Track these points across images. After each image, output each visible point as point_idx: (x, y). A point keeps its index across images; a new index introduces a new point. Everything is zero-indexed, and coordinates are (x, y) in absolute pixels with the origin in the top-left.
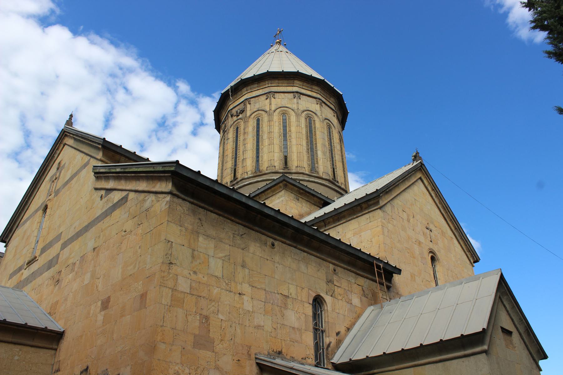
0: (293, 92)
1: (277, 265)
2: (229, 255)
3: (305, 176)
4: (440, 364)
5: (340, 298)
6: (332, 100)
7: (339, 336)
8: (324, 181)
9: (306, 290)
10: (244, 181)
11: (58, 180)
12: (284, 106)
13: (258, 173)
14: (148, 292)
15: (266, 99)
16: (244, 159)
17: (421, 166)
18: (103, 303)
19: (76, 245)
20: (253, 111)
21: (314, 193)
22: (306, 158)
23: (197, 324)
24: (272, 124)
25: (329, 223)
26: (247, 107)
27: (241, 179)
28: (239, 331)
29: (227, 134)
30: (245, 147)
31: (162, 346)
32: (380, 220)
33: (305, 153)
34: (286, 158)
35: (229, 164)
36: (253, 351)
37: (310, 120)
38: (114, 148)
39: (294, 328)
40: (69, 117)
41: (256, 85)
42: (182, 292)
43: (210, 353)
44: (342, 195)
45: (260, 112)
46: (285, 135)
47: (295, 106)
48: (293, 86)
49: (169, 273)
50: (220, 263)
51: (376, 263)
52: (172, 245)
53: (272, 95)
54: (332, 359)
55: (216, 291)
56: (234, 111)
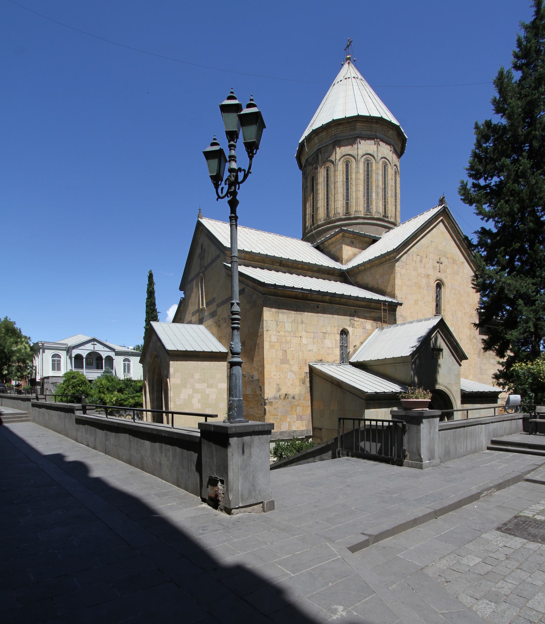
7: (355, 347)
11: (204, 259)
23: (281, 354)
36: (308, 361)
39: (329, 348)
42: (273, 342)
44: (389, 229)
49: (267, 335)
55: (288, 339)
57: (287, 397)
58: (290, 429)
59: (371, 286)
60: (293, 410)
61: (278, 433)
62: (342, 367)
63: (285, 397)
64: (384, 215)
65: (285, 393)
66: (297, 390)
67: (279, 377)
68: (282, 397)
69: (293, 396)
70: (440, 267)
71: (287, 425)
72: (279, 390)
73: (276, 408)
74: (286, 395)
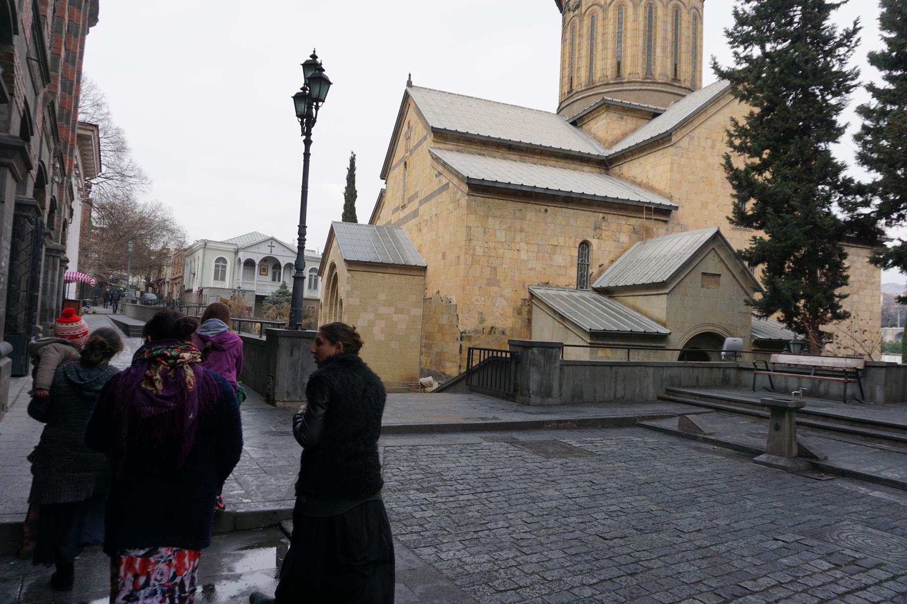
3: (638, 84)
4: (646, 297)
5: (608, 239)
20: (588, 6)
22: (640, 61)
23: (489, 272)
25: (635, 153)
28: (517, 273)
30: (579, 53)
32: (670, 157)
33: (640, 54)
34: (619, 64)
35: (567, 73)
36: (526, 285)
38: (440, 131)
39: (560, 267)
45: (595, 7)
46: (619, 38)
49: (469, 246)
50: (504, 232)
52: (470, 229)
57: (493, 331)
63: (491, 331)
65: (490, 325)
72: (482, 320)
74: (492, 328)
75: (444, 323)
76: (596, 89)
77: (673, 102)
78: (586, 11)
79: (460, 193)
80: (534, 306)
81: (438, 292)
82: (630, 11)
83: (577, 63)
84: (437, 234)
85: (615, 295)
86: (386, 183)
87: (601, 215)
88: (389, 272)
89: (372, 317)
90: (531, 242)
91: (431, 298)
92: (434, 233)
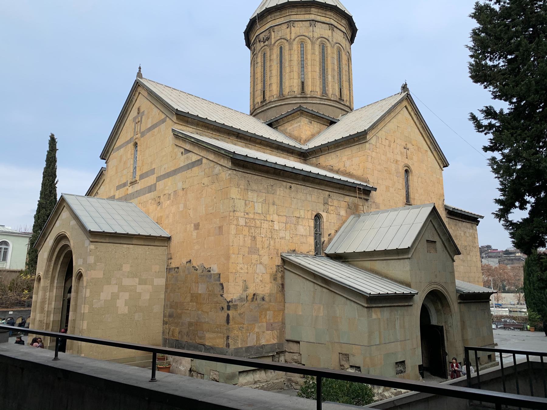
0: (310, 21)
1: (293, 199)
2: (265, 199)
6: (344, 22)
8: (332, 102)
9: (310, 211)
10: (271, 103)
11: (141, 123)
12: (302, 34)
13: (282, 97)
14: (223, 226)
15: (287, 28)
16: (270, 84)
17: (407, 96)
18: (195, 225)
19: (169, 181)
21: (323, 116)
22: (318, 83)
24: (293, 52)
26: (271, 35)
27: (269, 101)
29: (257, 58)
30: (271, 73)
31: (233, 256)
33: (318, 78)
34: (303, 83)
35: (259, 87)
36: (280, 252)
37: (323, 47)
40: (138, 70)
41: (278, 14)
43: (257, 256)
45: (283, 40)
47: (311, 34)
48: (309, 14)
51: (358, 187)
52: (234, 200)
53: (292, 24)
54: (325, 250)
56: (262, 36)
57: (255, 298)
58: (258, 342)
59: (337, 169)
60: (263, 317)
61: (244, 349)
62: (318, 259)
64: (339, 98)
66: (267, 288)
67: (246, 271)
68: (250, 298)
69: (262, 296)
70: (406, 153)
71: (255, 336)
72: (246, 288)
73: (242, 314)
74: (254, 295)
75: (200, 292)
76: (286, 100)
77: (341, 115)
78: (275, 43)
79: (218, 168)
80: (286, 271)
81: (190, 261)
82: (309, 46)
83: (269, 80)
84: (185, 206)
85: (349, 260)
86: (106, 163)
87: (327, 193)
88: (133, 243)
89: (115, 289)
90: (281, 214)
91: (178, 268)
92: (181, 206)
